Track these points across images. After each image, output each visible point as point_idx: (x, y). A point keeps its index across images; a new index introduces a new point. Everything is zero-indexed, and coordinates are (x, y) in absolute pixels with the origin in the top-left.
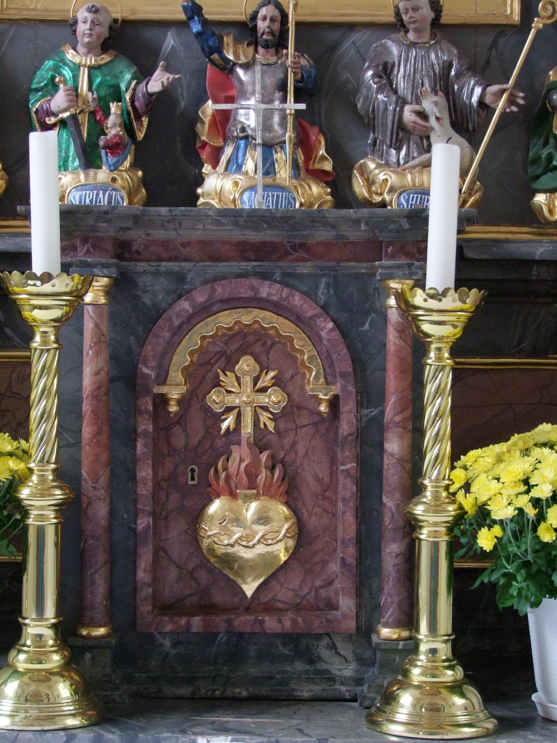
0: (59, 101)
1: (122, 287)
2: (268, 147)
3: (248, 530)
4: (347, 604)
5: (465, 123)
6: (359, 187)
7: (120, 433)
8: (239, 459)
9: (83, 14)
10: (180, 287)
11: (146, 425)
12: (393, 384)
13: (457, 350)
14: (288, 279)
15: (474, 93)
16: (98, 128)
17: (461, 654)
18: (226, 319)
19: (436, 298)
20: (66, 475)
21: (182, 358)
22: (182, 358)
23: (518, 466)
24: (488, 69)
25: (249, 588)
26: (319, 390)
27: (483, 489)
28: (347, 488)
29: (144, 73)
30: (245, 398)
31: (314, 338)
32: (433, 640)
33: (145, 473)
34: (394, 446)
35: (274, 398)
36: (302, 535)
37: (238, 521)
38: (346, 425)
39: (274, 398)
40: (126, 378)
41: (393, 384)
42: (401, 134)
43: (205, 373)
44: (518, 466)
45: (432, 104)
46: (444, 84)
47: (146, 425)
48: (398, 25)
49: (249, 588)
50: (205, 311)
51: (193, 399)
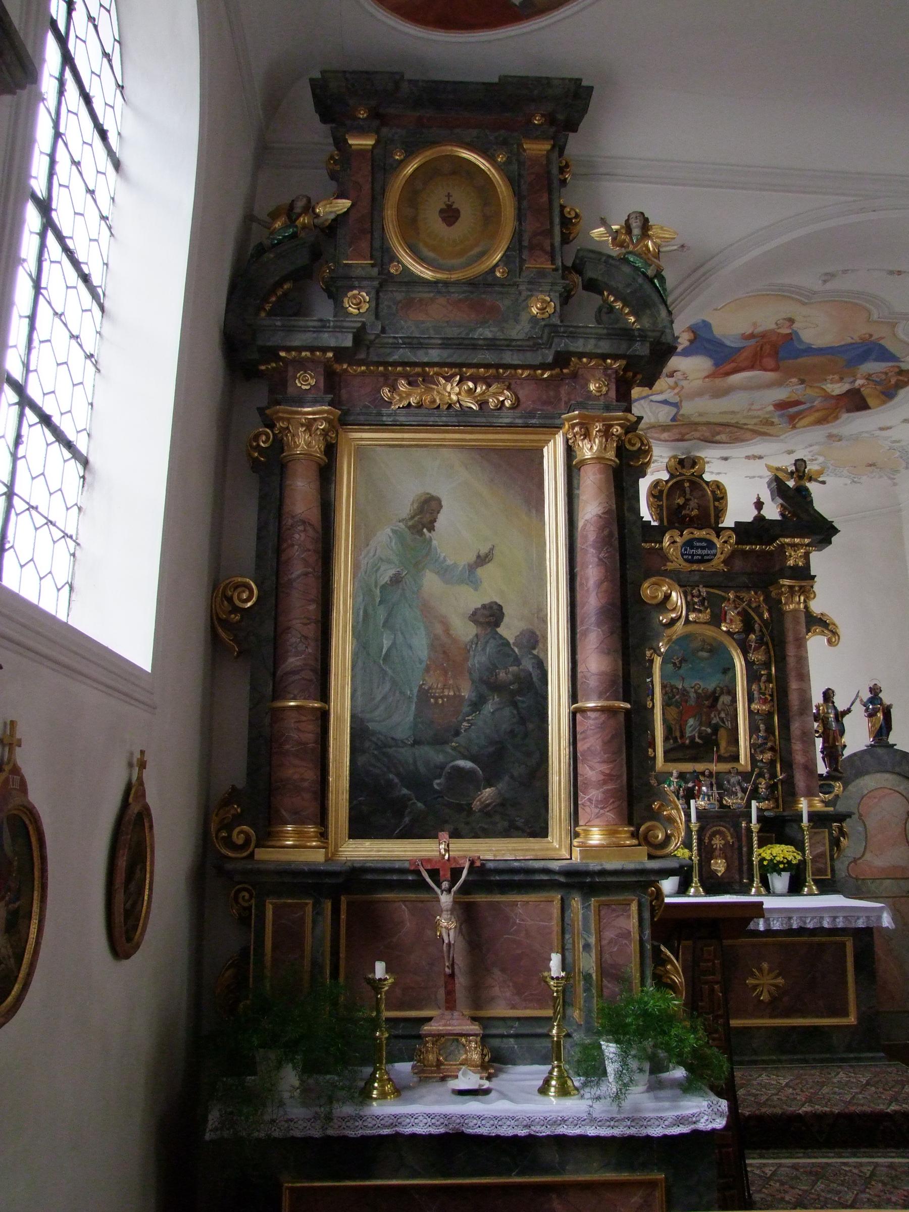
3: (719, 866)
4: (737, 876)
6: (724, 802)
8: (717, 853)
9: (674, 771)
12: (744, 839)
14: (725, 821)
16: (678, 793)
17: (761, 882)
18: (715, 829)
19: (755, 825)
23: (769, 852)
25: (719, 874)
27: (764, 855)
28: (736, 856)
29: (687, 783)
30: (718, 842)
31: (729, 830)
34: (745, 849)
35: (723, 842)
37: (717, 863)
38: (736, 846)
39: (723, 842)
41: (744, 839)
44: (769, 852)
45: (738, 788)
46: (739, 783)
49: (719, 874)
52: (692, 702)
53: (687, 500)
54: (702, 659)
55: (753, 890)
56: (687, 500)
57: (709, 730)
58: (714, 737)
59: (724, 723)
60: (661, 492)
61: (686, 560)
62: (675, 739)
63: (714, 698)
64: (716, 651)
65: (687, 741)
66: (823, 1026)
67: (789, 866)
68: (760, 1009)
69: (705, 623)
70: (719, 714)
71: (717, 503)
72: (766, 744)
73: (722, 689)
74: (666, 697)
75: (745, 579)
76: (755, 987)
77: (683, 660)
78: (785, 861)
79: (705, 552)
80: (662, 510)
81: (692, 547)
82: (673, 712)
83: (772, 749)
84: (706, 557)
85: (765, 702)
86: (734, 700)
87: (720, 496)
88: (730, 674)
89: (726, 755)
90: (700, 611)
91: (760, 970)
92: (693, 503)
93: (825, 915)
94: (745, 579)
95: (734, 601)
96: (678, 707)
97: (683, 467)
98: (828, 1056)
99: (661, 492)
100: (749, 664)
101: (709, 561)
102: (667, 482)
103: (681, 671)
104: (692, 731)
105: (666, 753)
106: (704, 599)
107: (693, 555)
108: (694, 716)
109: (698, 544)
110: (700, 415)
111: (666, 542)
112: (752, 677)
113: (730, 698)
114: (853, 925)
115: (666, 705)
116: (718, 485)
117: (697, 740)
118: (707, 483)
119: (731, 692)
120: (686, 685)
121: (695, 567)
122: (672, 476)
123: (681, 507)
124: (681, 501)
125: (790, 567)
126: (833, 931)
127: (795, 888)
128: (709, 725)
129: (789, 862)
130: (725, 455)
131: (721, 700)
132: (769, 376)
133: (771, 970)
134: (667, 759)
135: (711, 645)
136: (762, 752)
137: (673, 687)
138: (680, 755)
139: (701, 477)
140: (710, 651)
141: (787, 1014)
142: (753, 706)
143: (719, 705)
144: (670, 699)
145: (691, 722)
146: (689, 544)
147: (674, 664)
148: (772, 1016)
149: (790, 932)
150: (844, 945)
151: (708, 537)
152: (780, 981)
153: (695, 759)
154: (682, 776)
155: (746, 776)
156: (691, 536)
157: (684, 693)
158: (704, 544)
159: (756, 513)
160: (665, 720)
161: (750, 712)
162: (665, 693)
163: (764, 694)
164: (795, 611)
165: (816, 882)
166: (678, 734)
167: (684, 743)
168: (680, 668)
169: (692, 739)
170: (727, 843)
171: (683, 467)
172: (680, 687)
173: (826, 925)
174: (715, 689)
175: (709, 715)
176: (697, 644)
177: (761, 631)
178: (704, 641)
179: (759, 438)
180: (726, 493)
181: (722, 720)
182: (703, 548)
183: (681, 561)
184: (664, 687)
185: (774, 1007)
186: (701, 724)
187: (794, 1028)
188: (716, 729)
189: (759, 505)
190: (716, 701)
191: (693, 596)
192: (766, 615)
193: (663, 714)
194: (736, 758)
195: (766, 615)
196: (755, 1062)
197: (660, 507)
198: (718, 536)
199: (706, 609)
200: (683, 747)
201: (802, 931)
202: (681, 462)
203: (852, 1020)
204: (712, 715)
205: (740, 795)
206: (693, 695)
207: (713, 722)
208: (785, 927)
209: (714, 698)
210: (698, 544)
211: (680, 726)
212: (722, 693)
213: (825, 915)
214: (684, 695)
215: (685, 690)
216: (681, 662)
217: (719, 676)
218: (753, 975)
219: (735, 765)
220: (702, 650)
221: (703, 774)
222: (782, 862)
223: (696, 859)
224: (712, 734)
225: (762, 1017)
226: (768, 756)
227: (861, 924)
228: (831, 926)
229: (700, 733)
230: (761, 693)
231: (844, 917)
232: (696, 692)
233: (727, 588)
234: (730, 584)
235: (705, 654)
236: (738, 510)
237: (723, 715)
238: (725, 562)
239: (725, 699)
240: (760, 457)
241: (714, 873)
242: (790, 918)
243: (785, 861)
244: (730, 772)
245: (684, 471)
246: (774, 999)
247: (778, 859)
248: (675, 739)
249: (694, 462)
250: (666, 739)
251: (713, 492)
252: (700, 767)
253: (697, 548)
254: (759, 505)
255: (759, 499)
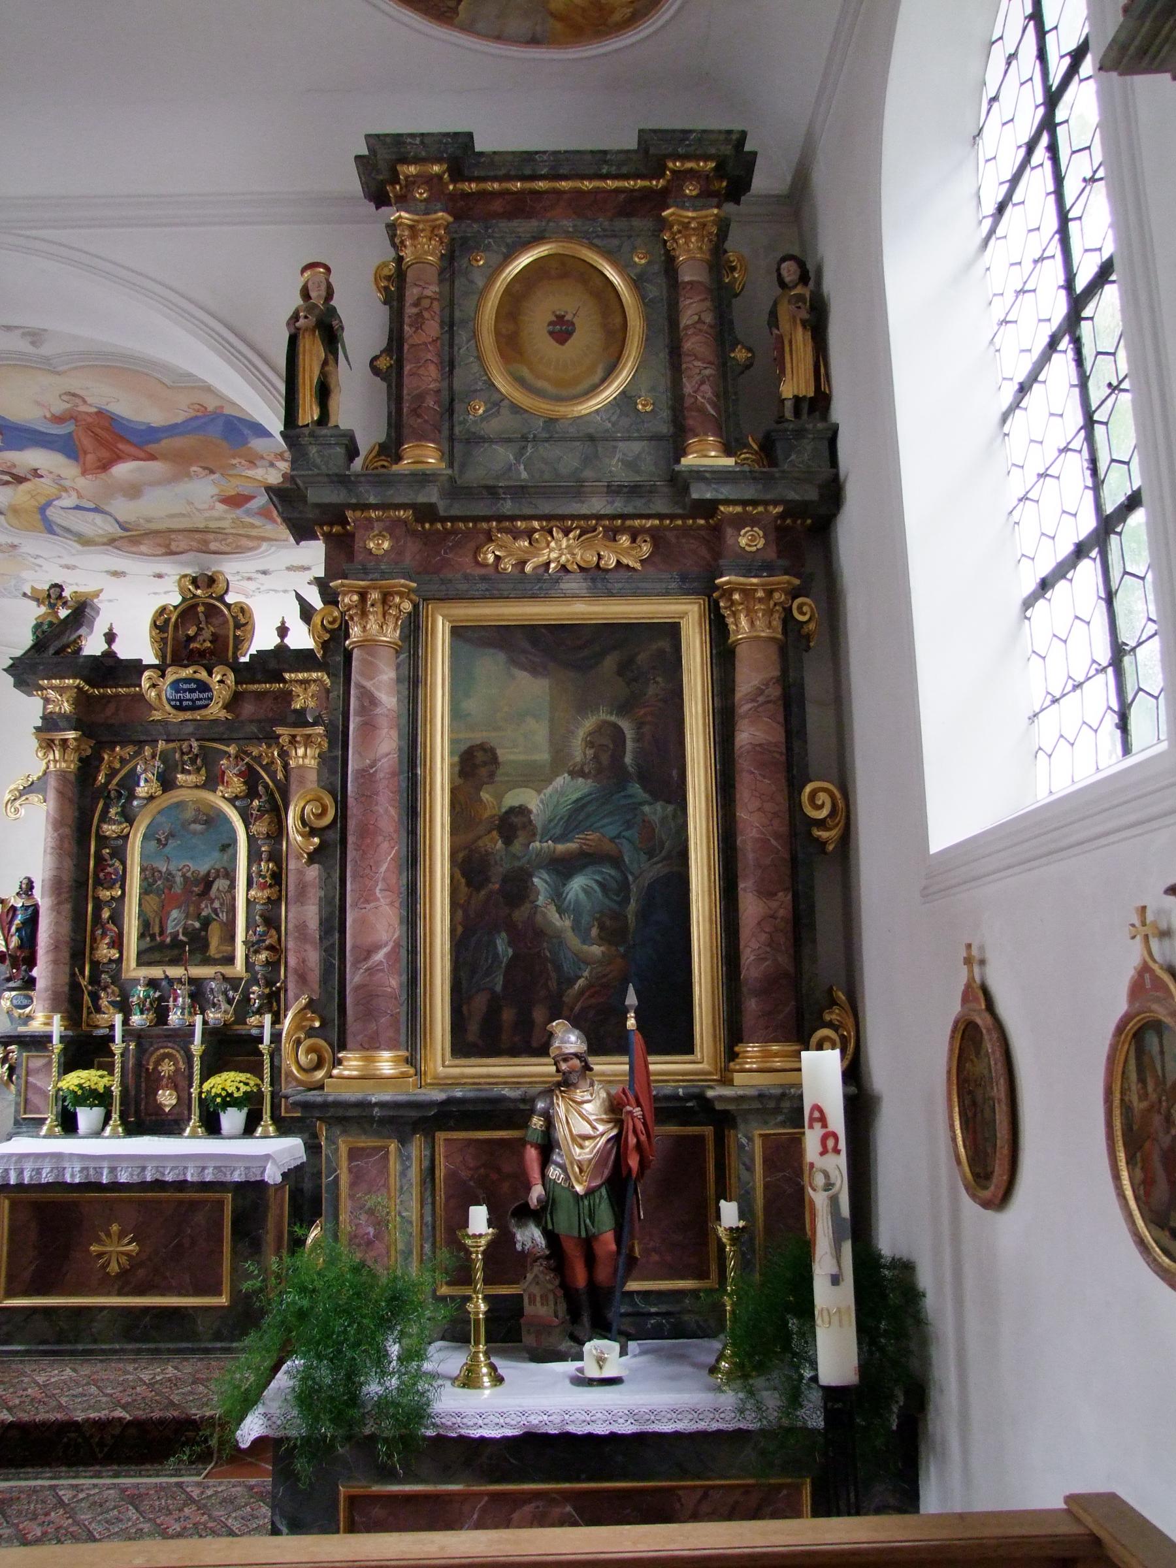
0: (135, 999)
1: (138, 1045)
2: (183, 1009)
3: (167, 1098)
5: (229, 1001)
7: (138, 1076)
8: (165, 1081)
10: (151, 1044)
11: (144, 1075)
13: (201, 1057)
14: (174, 1042)
15: (231, 993)
16: (144, 1005)
17: (200, 1120)
18: (162, 1051)
19: (197, 1047)
20: (123, 1083)
21: (153, 1059)
22: (153, 1059)
24: (235, 990)
25: (167, 1110)
26: (182, 1066)
30: (167, 1068)
32: (195, 1118)
33: (143, 1085)
36: (179, 1098)
39: (172, 1068)
40: (139, 1064)
42: (214, 1005)
43: (158, 1062)
46: (225, 993)
47: (144, 1075)
48: (213, 979)
49: (167, 1110)
50: (158, 1049)
51: (155, 1069)
52: (178, 889)
53: (200, 629)
54: (195, 833)
55: (188, 1130)
56: (200, 629)
57: (197, 925)
58: (203, 933)
59: (217, 915)
60: (167, 621)
61: (174, 707)
62: (153, 937)
63: (207, 883)
64: (213, 820)
65: (168, 940)
66: (186, 1308)
67: (230, 1101)
68: (106, 1284)
69: (197, 787)
70: (212, 903)
71: (238, 633)
72: (264, 941)
73: (218, 871)
74: (145, 884)
75: (254, 728)
76: (100, 1255)
77: (171, 835)
78: (224, 1093)
79: (196, 695)
80: (165, 644)
81: (177, 691)
82: (153, 901)
83: (271, 948)
84: (198, 703)
85: (263, 887)
86: (232, 886)
87: (243, 621)
88: (230, 851)
89: (217, 956)
90: (189, 772)
91: (109, 1235)
92: (206, 634)
93: (190, 1165)
94: (254, 728)
95: (236, 757)
96: (159, 896)
97: (197, 587)
98: (190, 1345)
99: (167, 621)
100: (251, 839)
101: (206, 706)
102: (176, 607)
103: (167, 849)
104: (176, 925)
105: (139, 954)
106: (197, 756)
107: (181, 701)
108: (179, 907)
109: (185, 686)
110: (149, 521)
111: (145, 684)
112: (254, 856)
113: (228, 882)
114: (228, 1179)
115: (145, 891)
116: (243, 610)
117: (181, 937)
118: (228, 606)
119: (230, 876)
120: (172, 868)
121: (188, 715)
122: (184, 600)
123: (190, 639)
124: (191, 632)
125: (296, 711)
126: (204, 1186)
127: (249, 1130)
128: (198, 917)
129: (230, 1095)
130: (261, 568)
131: (215, 887)
132: (156, 468)
133: (122, 1234)
134: (140, 963)
135: (207, 815)
136: (257, 952)
137: (154, 870)
138: (157, 956)
139: (221, 599)
140: (206, 822)
141: (141, 1292)
142: (252, 893)
143: (213, 892)
144: (150, 885)
145: (175, 914)
146: (175, 684)
147: (159, 840)
148: (120, 1294)
149: (143, 1186)
150: (221, 1203)
151: (197, 676)
152: (133, 1247)
153: (174, 962)
154: (152, 983)
155: (234, 982)
156: (175, 677)
157: (169, 877)
158: (193, 686)
159: (278, 640)
160: (141, 913)
161: (248, 900)
162: (144, 879)
163: (264, 877)
164: (300, 767)
165: (276, 1119)
166: (157, 930)
167: (163, 942)
168: (165, 845)
169: (175, 936)
170: (177, 1070)
171: (197, 587)
172: (164, 870)
173: (189, 1179)
174: (209, 873)
175: (198, 906)
176: (189, 814)
177: (271, 795)
178: (198, 810)
179: (265, 545)
180: (251, 616)
181: (215, 911)
182: (191, 691)
183: (168, 707)
184: (143, 870)
185: (125, 1282)
186: (187, 917)
187: (146, 1310)
188: (206, 923)
189: (283, 631)
190: (205, 886)
191: (183, 753)
192: (280, 776)
193: (140, 905)
194: (230, 960)
195: (280, 776)
196: (90, 1352)
197: (164, 641)
198: (210, 674)
199: (198, 770)
200: (162, 947)
201: (159, 1185)
202: (194, 581)
203: (223, 1300)
204: (203, 906)
205: (224, 1006)
206: (179, 880)
207: (204, 914)
208: (136, 1179)
209: (207, 883)
210: (185, 686)
211: (161, 922)
212: (217, 876)
213: (190, 1165)
214: (168, 880)
215: (170, 874)
216: (167, 839)
217: (216, 854)
218: (99, 1241)
219: (227, 971)
220: (194, 822)
221: (179, 981)
222: (220, 1095)
223: (116, 1090)
224: (201, 929)
225: (108, 1294)
226: (263, 956)
227: (237, 1177)
228: (195, 1179)
229: (185, 929)
230: (261, 876)
231: (215, 1168)
232: (184, 876)
233: (227, 741)
234: (235, 736)
235: (198, 827)
236: (263, 640)
237: (217, 905)
238: (227, 707)
239: (221, 884)
240: (308, 569)
241: (160, 1107)
242: (144, 1169)
243: (224, 1093)
244: (213, 979)
245: (199, 592)
246: (124, 1273)
247: (214, 1091)
248: (153, 937)
249: (212, 581)
250: (141, 936)
251: (235, 618)
252: (175, 972)
253: (185, 691)
254: (283, 631)
255: (283, 623)
